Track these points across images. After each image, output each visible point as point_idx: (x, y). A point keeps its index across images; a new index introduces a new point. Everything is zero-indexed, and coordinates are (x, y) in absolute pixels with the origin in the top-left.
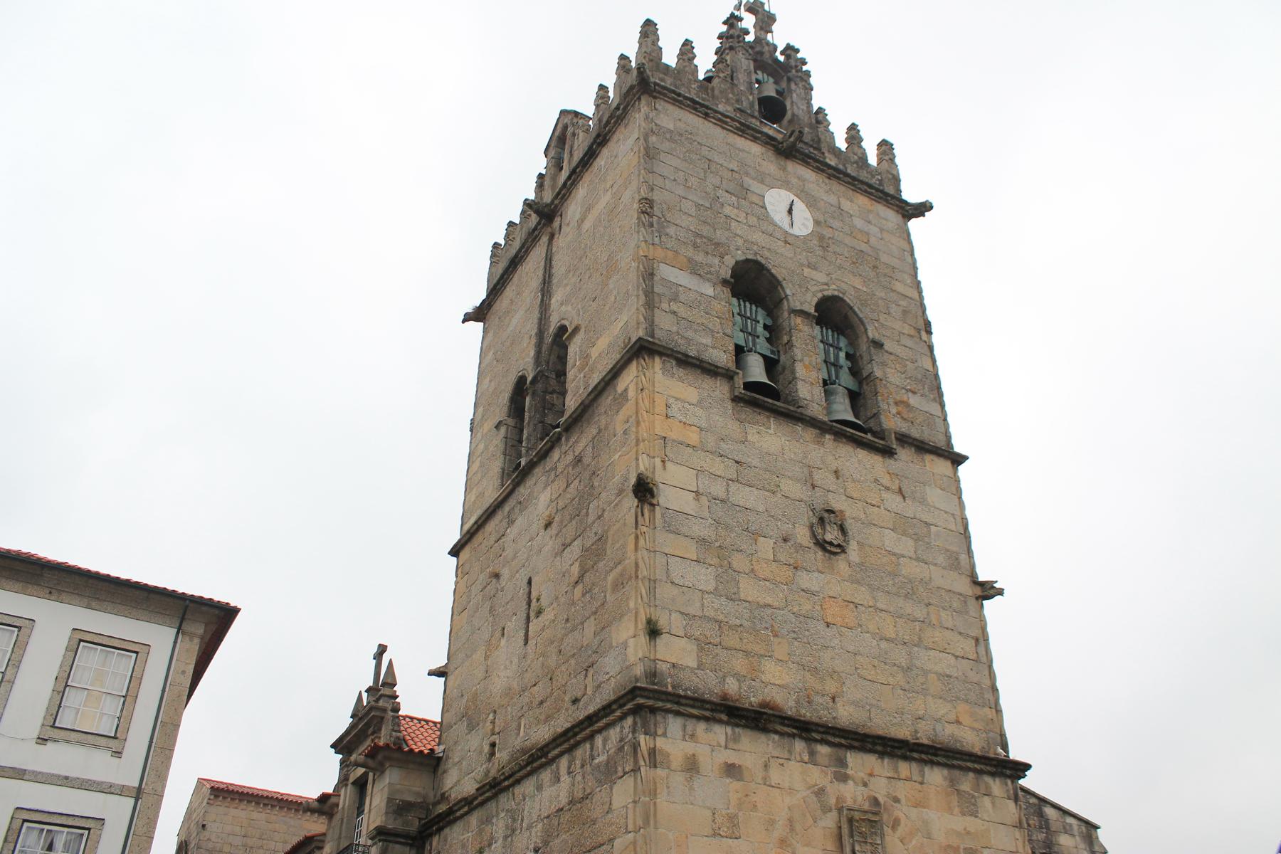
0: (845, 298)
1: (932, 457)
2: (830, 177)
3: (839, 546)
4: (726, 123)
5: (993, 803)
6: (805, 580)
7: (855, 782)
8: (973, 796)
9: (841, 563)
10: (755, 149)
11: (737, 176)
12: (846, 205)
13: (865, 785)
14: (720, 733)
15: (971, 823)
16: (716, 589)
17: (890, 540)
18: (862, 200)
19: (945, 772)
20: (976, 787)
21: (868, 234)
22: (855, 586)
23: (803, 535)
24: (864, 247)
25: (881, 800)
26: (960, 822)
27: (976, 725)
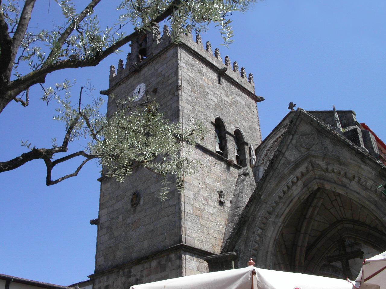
3: (135, 204)
5: (171, 264)
6: (129, 221)
7: (133, 277)
8: (165, 264)
9: (139, 209)
10: (132, 79)
13: (135, 276)
16: (109, 239)
19: (158, 260)
20: (166, 261)
21: (161, 71)
22: (141, 213)
23: (129, 207)
24: (160, 79)
25: (138, 278)
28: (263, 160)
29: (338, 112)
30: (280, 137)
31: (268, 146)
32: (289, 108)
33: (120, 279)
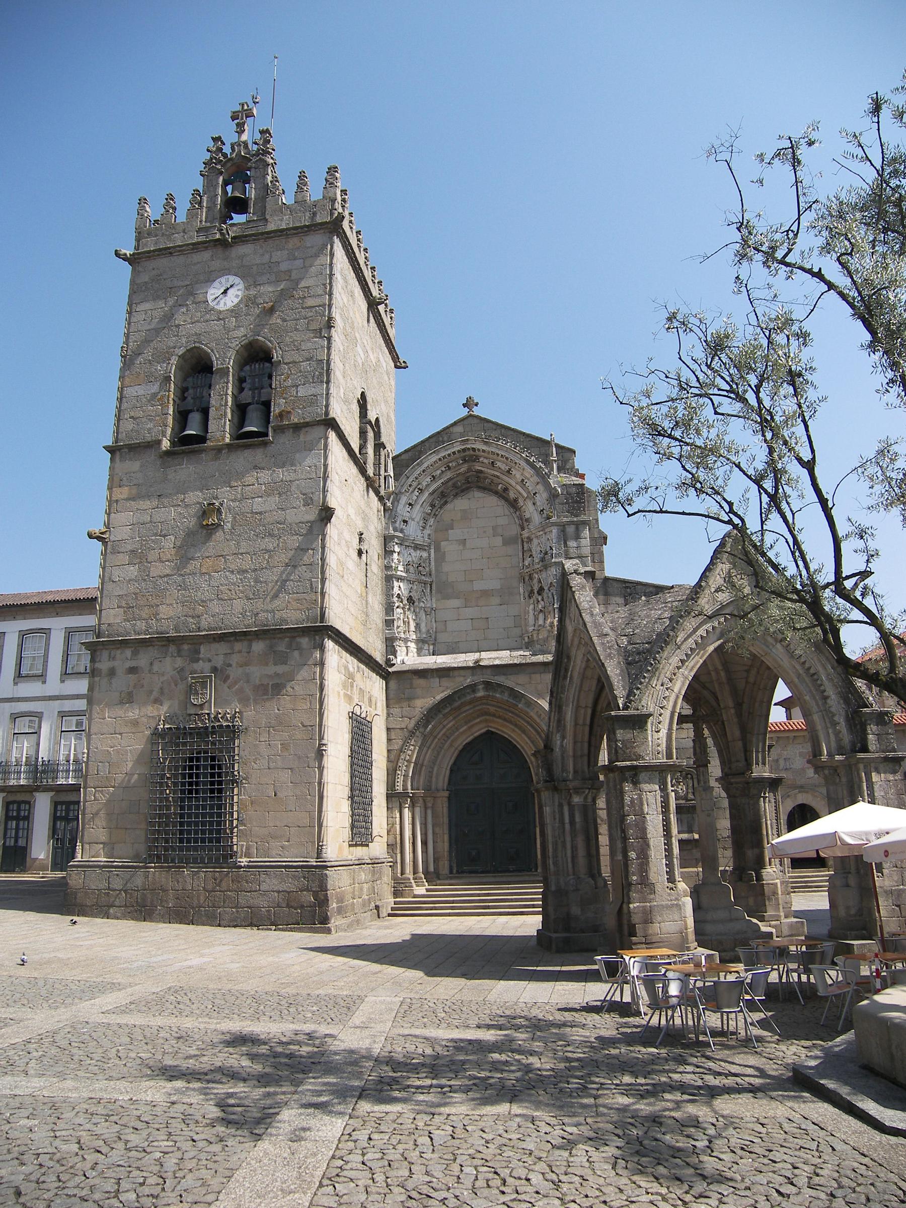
0: (260, 338)
1: (307, 429)
2: (266, 239)
4: (184, 250)
5: (301, 654)
8: (286, 653)
9: (219, 535)
10: (206, 255)
11: (189, 287)
12: (277, 256)
13: (210, 661)
14: (128, 653)
15: (280, 669)
17: (258, 504)
18: (293, 242)
19: (268, 642)
20: (289, 646)
21: (290, 271)
25: (219, 668)
26: (271, 669)
27: (301, 607)
28: (410, 486)
29: (557, 446)
30: (449, 455)
31: (425, 465)
32: (464, 405)
33: (168, 659)
